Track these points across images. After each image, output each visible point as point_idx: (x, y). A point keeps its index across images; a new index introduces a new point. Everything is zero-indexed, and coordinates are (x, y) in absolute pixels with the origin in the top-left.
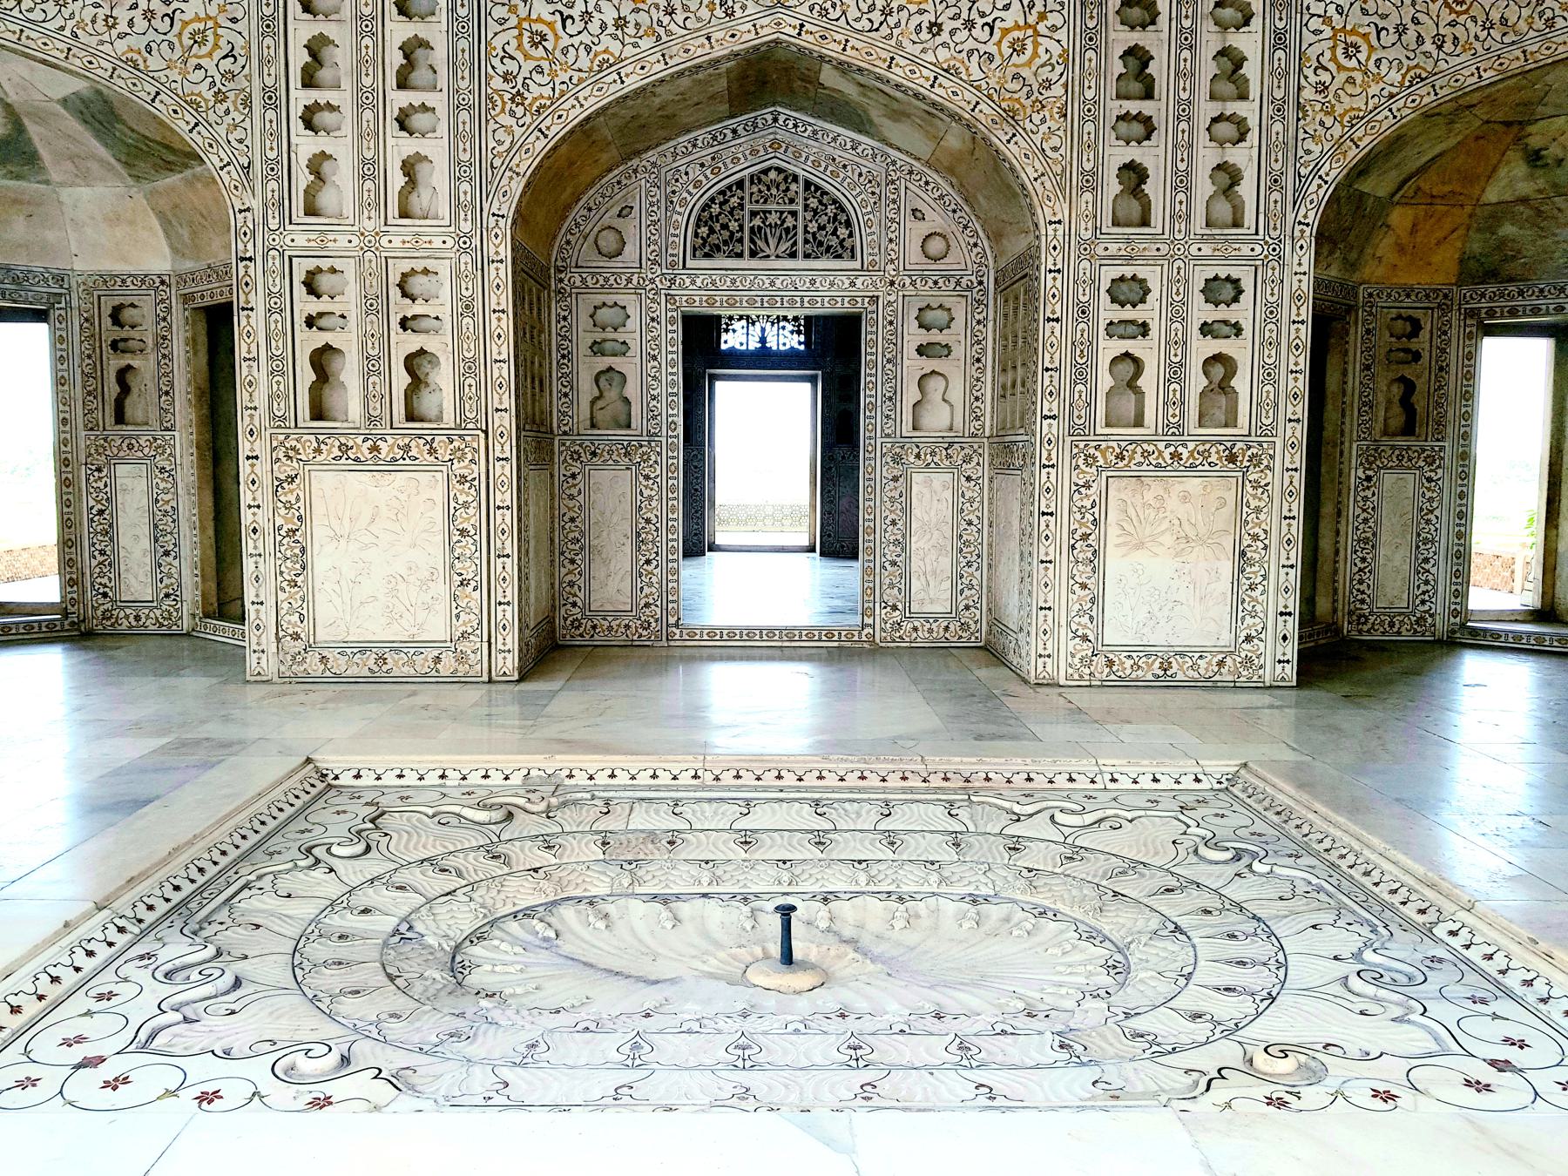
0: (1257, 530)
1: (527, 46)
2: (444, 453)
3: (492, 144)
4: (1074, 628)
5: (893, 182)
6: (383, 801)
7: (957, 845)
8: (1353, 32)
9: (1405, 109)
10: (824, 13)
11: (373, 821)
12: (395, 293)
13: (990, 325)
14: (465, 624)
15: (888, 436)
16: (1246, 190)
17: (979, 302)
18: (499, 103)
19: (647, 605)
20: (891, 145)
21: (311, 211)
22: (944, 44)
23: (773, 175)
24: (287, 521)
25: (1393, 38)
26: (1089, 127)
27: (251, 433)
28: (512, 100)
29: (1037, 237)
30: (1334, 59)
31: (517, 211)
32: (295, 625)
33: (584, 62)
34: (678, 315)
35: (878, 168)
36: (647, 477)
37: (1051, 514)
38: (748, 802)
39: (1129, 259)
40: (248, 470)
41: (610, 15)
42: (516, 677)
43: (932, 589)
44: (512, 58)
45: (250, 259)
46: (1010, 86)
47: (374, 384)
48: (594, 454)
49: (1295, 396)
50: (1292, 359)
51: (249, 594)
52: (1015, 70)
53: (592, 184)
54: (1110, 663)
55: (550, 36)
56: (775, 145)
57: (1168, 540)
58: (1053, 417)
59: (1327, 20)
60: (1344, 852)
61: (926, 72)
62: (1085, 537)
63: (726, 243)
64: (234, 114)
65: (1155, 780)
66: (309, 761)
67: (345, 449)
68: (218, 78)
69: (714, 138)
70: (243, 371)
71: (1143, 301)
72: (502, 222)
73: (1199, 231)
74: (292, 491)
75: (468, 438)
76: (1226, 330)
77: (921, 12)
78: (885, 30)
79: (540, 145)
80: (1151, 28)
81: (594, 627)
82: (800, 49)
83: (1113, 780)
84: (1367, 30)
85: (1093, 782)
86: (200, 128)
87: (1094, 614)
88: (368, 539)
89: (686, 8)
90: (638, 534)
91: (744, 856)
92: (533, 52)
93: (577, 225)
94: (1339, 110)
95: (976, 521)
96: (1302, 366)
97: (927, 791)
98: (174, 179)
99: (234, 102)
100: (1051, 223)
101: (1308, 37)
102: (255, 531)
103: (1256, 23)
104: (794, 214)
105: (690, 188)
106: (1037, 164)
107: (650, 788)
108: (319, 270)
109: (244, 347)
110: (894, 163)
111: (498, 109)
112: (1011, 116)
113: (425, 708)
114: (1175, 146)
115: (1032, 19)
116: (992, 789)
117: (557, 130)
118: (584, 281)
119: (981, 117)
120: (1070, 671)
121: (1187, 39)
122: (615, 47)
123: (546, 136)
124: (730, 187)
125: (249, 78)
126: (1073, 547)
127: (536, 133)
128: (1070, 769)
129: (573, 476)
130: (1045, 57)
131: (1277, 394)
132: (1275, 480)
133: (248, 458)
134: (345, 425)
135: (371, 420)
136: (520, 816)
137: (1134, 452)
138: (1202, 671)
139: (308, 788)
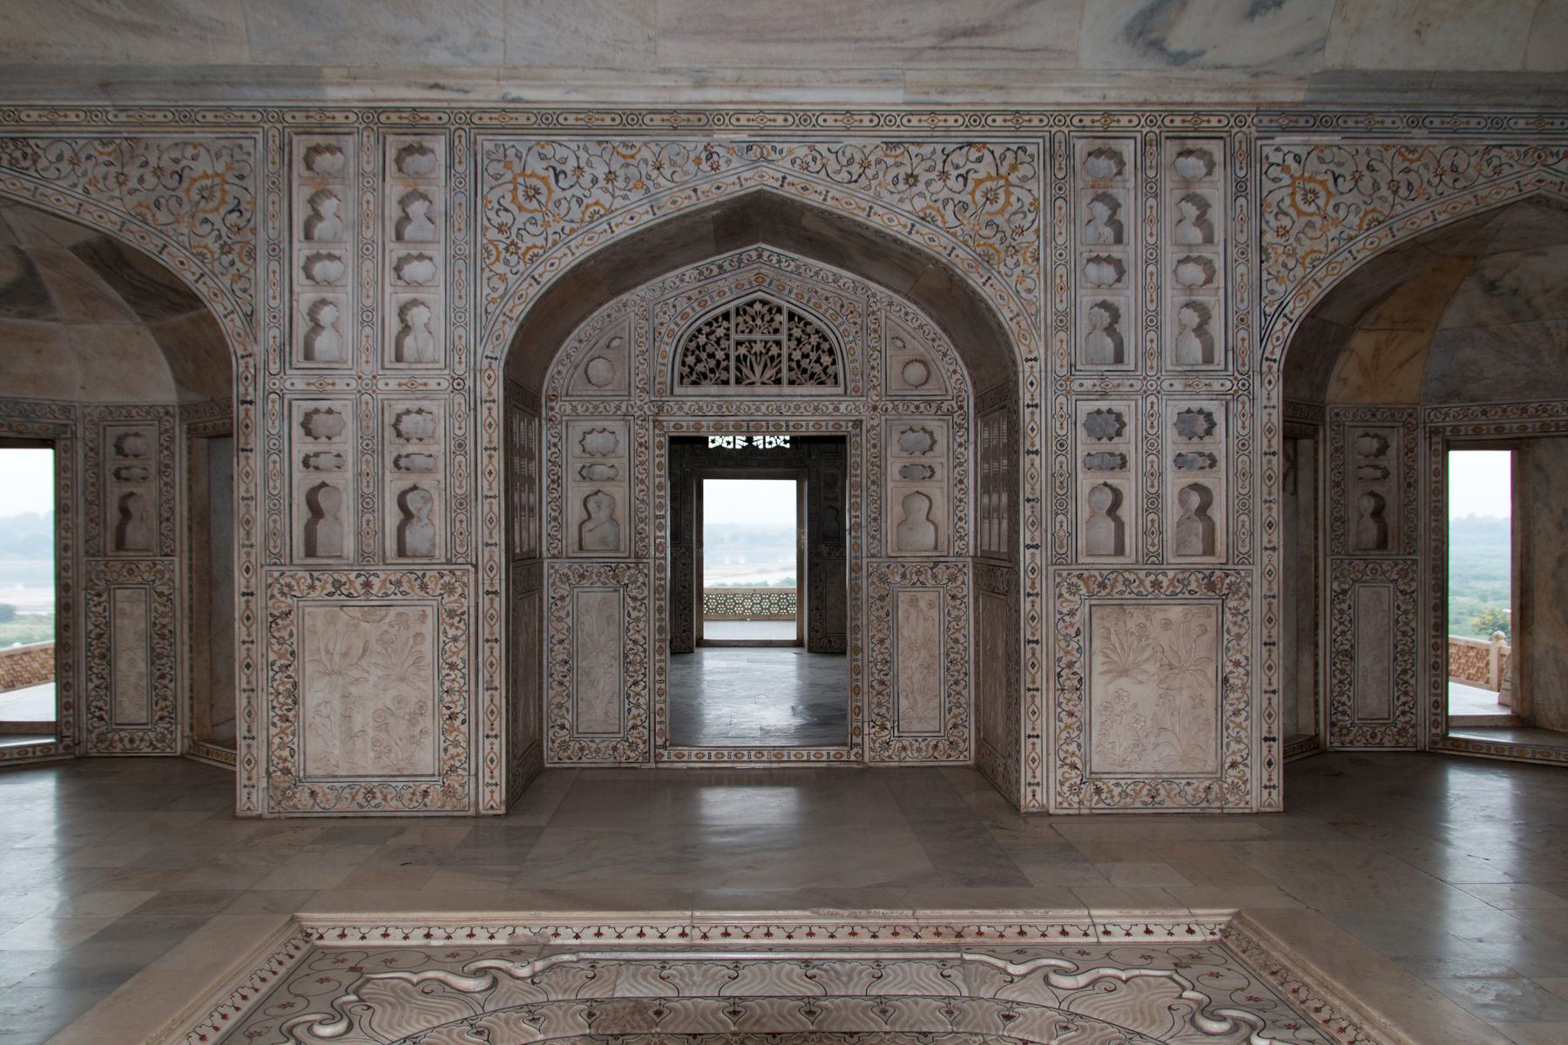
0: (1238, 657)
1: (521, 198)
2: (435, 587)
3: (486, 291)
4: (1062, 755)
5: (874, 313)
6: (366, 965)
7: (950, 1012)
8: (1310, 179)
9: (1364, 250)
11: (356, 992)
12: (389, 433)
13: (971, 448)
14: (452, 758)
15: (873, 556)
16: (1216, 327)
17: (960, 426)
18: (494, 252)
20: (871, 279)
21: (309, 356)
22: (920, 194)
23: (758, 306)
24: (281, 656)
25: (1350, 185)
26: (1061, 271)
28: (507, 250)
29: (1016, 373)
30: (1293, 205)
31: (510, 352)
32: (285, 760)
33: (576, 212)
36: (634, 599)
37: (1037, 642)
38: (737, 961)
39: (1104, 395)
40: (243, 606)
41: (601, 171)
42: (502, 810)
43: (921, 714)
44: (506, 210)
45: (251, 403)
46: (984, 232)
48: (582, 576)
49: (1270, 525)
50: (1265, 489)
51: (241, 729)
52: (988, 218)
53: (584, 318)
54: (1098, 791)
55: (544, 190)
56: (760, 278)
57: (1152, 667)
58: (1036, 547)
59: (1285, 168)
60: (1344, 1024)
61: (903, 220)
62: (1070, 665)
63: (712, 371)
64: (239, 265)
65: (1148, 932)
66: (293, 920)
67: (338, 585)
68: (224, 231)
69: (701, 273)
70: (241, 509)
71: (1119, 433)
73: (1170, 367)
74: (285, 627)
76: (1201, 462)
77: (898, 165)
78: (863, 182)
80: (1119, 178)
81: (582, 749)
82: (785, 203)
83: (1107, 933)
84: (1324, 177)
85: (1086, 935)
86: (206, 279)
87: (1081, 741)
88: (355, 673)
89: (673, 163)
90: (626, 656)
91: (733, 1028)
92: (528, 205)
93: (568, 356)
94: (1300, 252)
95: (962, 640)
96: (1275, 496)
97: (919, 948)
98: (179, 319)
99: (240, 255)
100: (1027, 360)
101: (1268, 185)
102: (248, 666)
103: (1219, 172)
104: (778, 343)
105: (678, 320)
106: (1012, 305)
107: (637, 948)
108: (317, 411)
109: (243, 488)
110: (874, 295)
111: (493, 258)
112: (987, 259)
113: (413, 848)
114: (1144, 288)
116: (984, 945)
117: (549, 276)
118: (574, 408)
119: (958, 261)
120: (1059, 799)
121: (1151, 189)
122: (606, 199)
124: (716, 320)
125: (254, 231)
126: (1059, 675)
127: (530, 280)
128: (1061, 921)
129: (562, 598)
130: (1016, 206)
131: (1252, 523)
132: (1255, 607)
133: (244, 594)
135: (363, 555)
136: (506, 982)
137: (1116, 580)
138: (1189, 798)
139: (293, 951)
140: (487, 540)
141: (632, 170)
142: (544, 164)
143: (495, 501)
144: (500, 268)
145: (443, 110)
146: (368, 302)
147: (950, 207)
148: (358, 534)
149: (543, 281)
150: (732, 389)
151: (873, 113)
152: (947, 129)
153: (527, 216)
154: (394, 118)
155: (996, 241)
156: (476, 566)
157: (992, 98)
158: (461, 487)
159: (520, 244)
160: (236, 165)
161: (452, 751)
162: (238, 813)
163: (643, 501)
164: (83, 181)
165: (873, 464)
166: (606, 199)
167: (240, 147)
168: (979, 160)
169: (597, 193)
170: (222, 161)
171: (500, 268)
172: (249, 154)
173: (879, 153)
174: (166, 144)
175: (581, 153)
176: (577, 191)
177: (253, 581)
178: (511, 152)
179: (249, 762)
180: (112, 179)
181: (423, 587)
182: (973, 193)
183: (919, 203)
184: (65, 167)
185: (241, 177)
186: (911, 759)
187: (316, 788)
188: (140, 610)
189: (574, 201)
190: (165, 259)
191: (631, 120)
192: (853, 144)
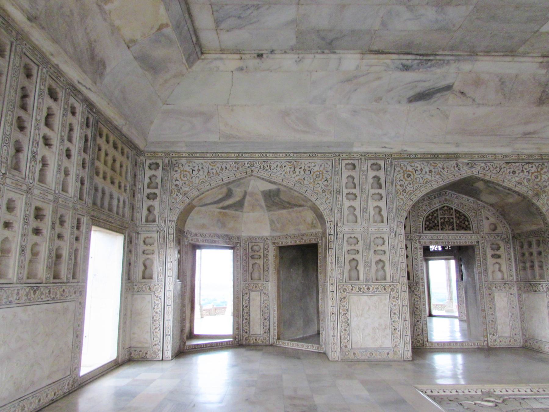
2: (389, 290)
10: (484, 169)
13: (512, 249)
19: (418, 335)
22: (517, 177)
23: (446, 208)
24: (344, 311)
27: (332, 284)
32: (346, 343)
33: (421, 181)
34: (422, 247)
35: (475, 206)
41: (427, 170)
42: (411, 359)
55: (412, 175)
63: (434, 226)
64: (327, 196)
67: (360, 289)
72: (401, 224)
77: (510, 168)
89: (447, 168)
90: (414, 313)
98: (284, 211)
108: (351, 237)
112: (537, 195)
115: (539, 170)
117: (415, 199)
122: (430, 178)
124: (434, 211)
130: (543, 180)
135: (367, 280)
141: (436, 170)
142: (412, 168)
145: (383, 153)
147: (525, 180)
148: (366, 274)
150: (440, 232)
151: (502, 154)
152: (523, 159)
154: (370, 155)
155: (539, 189)
157: (535, 151)
161: (395, 340)
162: (330, 359)
164: (284, 173)
165: (484, 254)
166: (430, 178)
168: (532, 167)
169: (427, 176)
171: (401, 197)
173: (504, 165)
174: (306, 163)
176: (421, 175)
177: (334, 288)
178: (402, 165)
179: (334, 344)
180: (291, 172)
181: (385, 289)
182: (531, 176)
183: (517, 179)
184: (279, 169)
185: (327, 171)
186: (503, 345)
187: (355, 352)
188: (259, 298)
190: (308, 195)
191: (435, 156)
192: (497, 163)
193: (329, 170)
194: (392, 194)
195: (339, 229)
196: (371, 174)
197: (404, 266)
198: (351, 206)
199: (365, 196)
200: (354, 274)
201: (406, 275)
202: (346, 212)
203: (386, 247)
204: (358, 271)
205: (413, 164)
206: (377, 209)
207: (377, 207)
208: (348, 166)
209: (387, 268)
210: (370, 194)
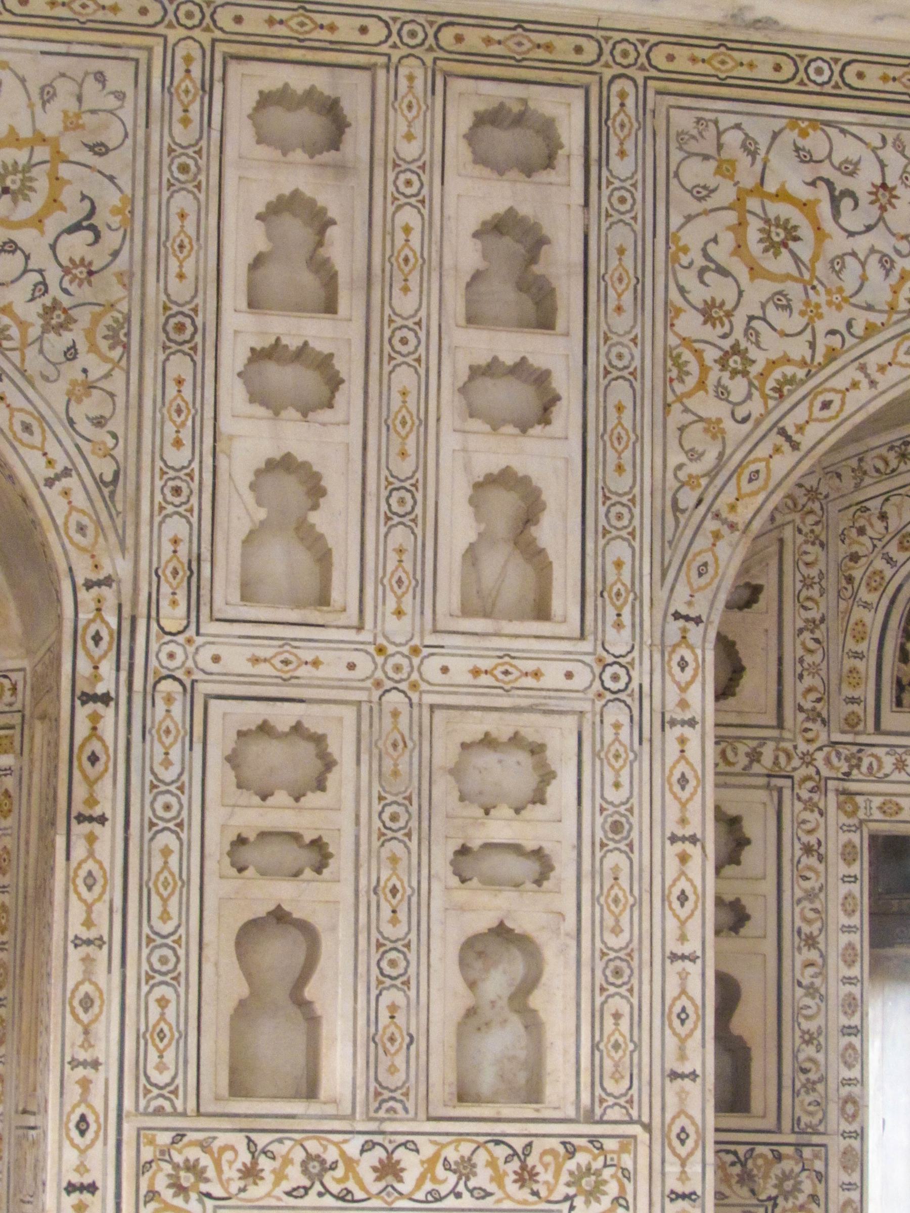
1: (755, 246)
3: (676, 457)
18: (694, 367)
27: (82, 1125)
28: (723, 362)
33: (878, 289)
44: (723, 271)
45: (105, 699)
47: (393, 1009)
55: (806, 231)
64: (86, 359)
68: (53, 275)
72: (695, 633)
75: (611, 1145)
79: (782, 463)
99: (90, 334)
105: (893, 550)
108: (265, 729)
109: (77, 911)
111: (691, 382)
123: (795, 446)
127: (775, 439)
133: (71, 1188)
134: (315, 1108)
140: (672, 1064)
142: (808, 172)
143: (694, 969)
144: (708, 406)
146: (404, 468)
149: (806, 440)
153: (767, 288)
154: (474, 39)
156: (648, 1128)
158: (616, 930)
159: (753, 353)
160: (86, 119)
163: (811, 990)
167: (100, 77)
170: (55, 107)
171: (708, 406)
172: (120, 96)
175: (890, 154)
176: (880, 240)
178: (733, 139)
181: (526, 1176)
185: (100, 149)
189: (874, 259)
193: (113, 137)
194: (633, 376)
195: (173, 655)
196: (473, 197)
197: (700, 988)
198: (284, 464)
199: (404, 377)
200: (276, 1043)
201: (702, 1057)
202: (240, 512)
203: (553, 826)
204: (312, 1021)
205: (816, 143)
206: (504, 503)
207: (505, 479)
208: (277, 117)
209: (555, 1001)
210: (455, 370)
